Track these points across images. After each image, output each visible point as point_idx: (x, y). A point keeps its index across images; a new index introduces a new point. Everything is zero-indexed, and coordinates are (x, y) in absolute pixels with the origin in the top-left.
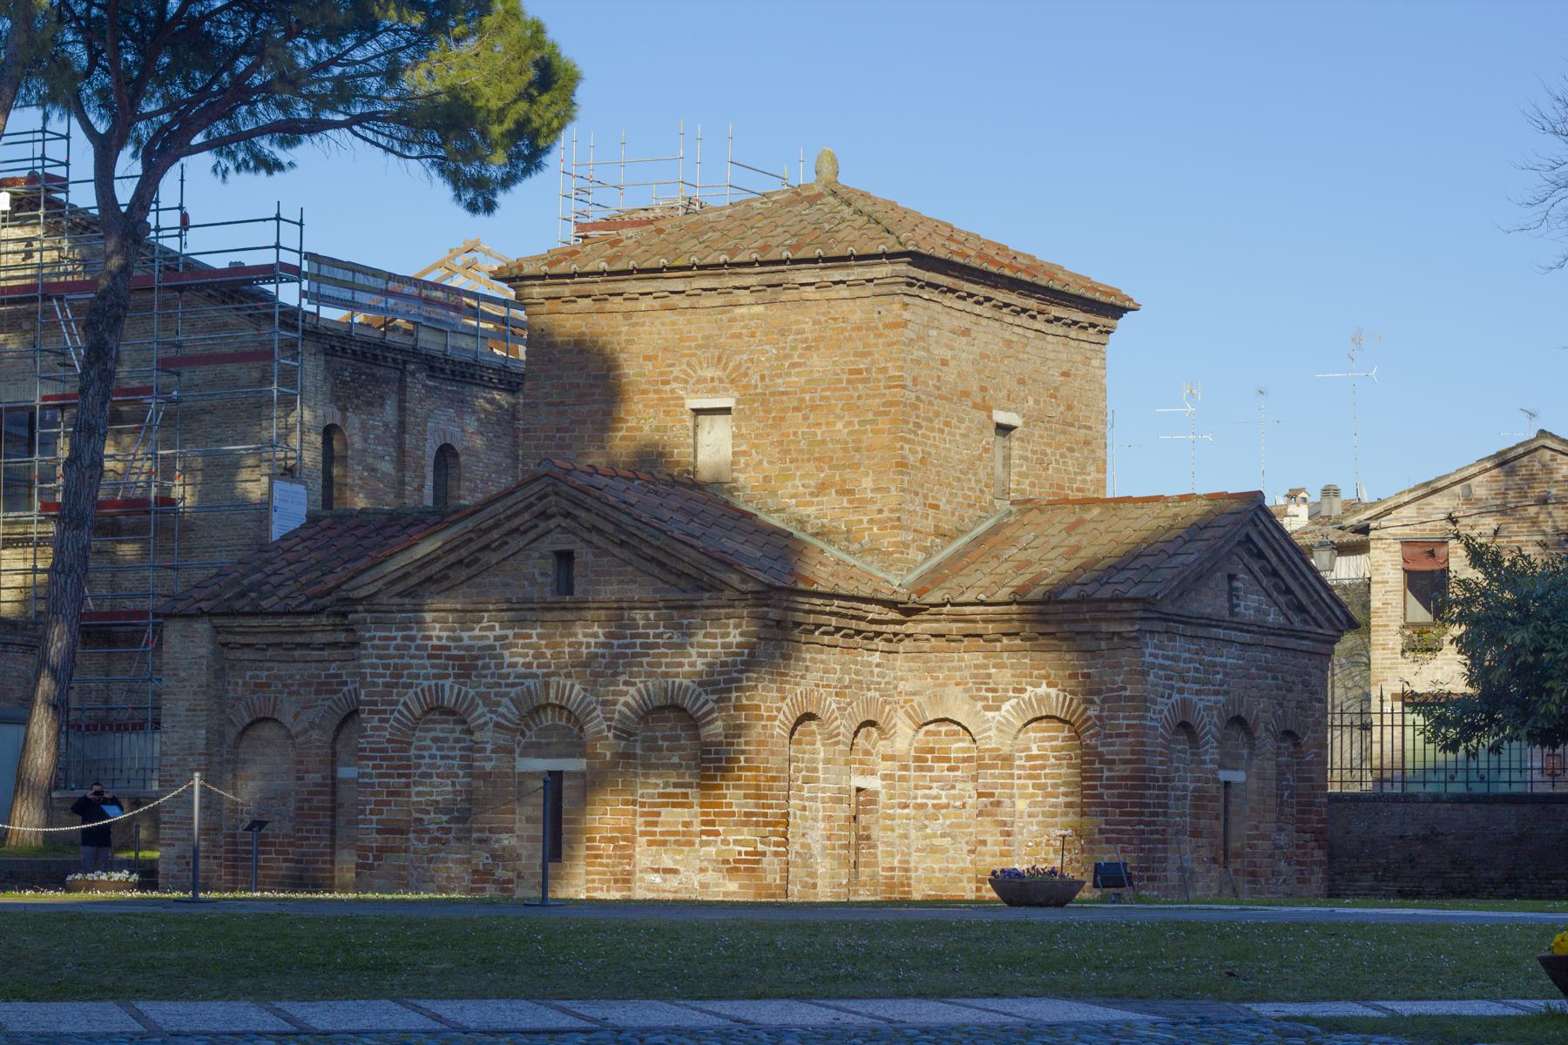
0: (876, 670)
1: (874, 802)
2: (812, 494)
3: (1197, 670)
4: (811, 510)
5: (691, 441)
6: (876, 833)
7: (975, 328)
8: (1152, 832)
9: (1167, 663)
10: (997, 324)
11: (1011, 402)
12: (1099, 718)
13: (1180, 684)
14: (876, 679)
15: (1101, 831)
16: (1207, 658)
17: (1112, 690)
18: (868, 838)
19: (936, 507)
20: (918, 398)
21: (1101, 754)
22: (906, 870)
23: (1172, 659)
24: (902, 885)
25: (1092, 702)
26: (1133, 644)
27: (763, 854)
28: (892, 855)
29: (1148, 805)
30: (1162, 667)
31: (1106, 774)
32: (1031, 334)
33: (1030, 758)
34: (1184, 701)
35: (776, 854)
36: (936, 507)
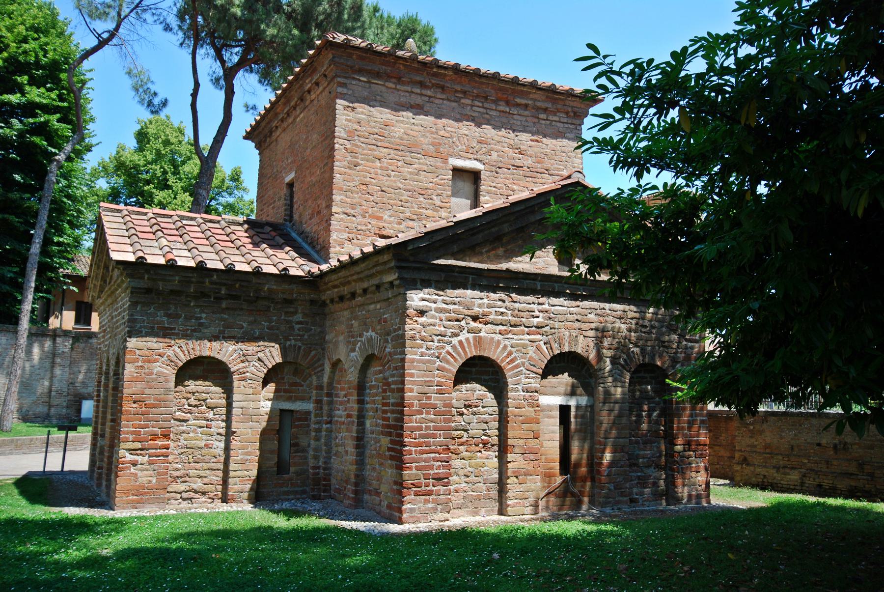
0: (297, 326)
1: (306, 419)
2: (310, 219)
3: (502, 314)
4: (308, 230)
5: (288, 202)
6: (303, 442)
7: (428, 105)
8: (422, 452)
9: (451, 307)
10: (454, 104)
11: (469, 152)
12: (390, 353)
13: (473, 324)
14: (297, 332)
15: (389, 449)
16: (517, 305)
17: (395, 330)
18: (296, 445)
19: (379, 218)
20: (356, 146)
21: (388, 384)
22: (325, 469)
23: (460, 303)
24: (325, 480)
25: (386, 341)
26: (402, 291)
27: (134, 464)
28: (316, 458)
29: (420, 429)
30: (441, 311)
31: (392, 401)
32: (494, 113)
33: (371, 387)
34: (479, 341)
35: (151, 463)
36: (379, 218)
